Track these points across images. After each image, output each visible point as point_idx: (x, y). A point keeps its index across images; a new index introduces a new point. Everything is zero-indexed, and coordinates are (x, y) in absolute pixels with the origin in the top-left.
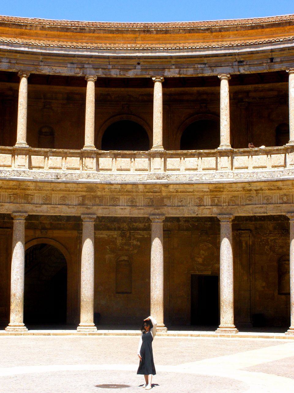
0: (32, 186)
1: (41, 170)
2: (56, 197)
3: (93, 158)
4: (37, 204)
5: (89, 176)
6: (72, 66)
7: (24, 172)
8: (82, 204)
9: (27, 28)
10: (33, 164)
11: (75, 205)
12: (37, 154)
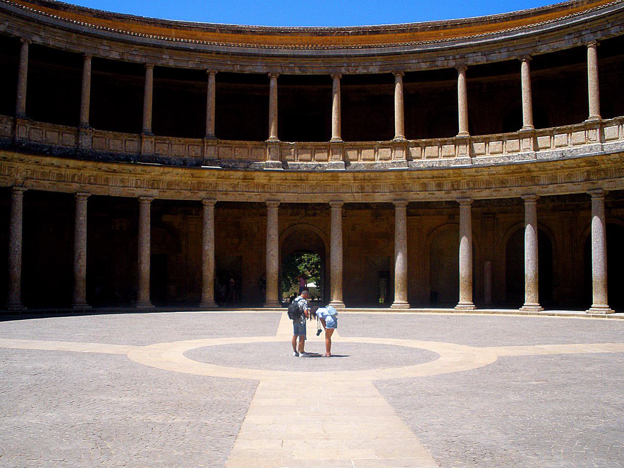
0: (532, 168)
1: (547, 151)
2: (561, 176)
3: (596, 129)
4: (544, 185)
5: (591, 149)
6: (570, 37)
7: (528, 154)
8: (587, 180)
9: (573, 6)
10: (540, 146)
11: (581, 182)
12: (543, 134)
